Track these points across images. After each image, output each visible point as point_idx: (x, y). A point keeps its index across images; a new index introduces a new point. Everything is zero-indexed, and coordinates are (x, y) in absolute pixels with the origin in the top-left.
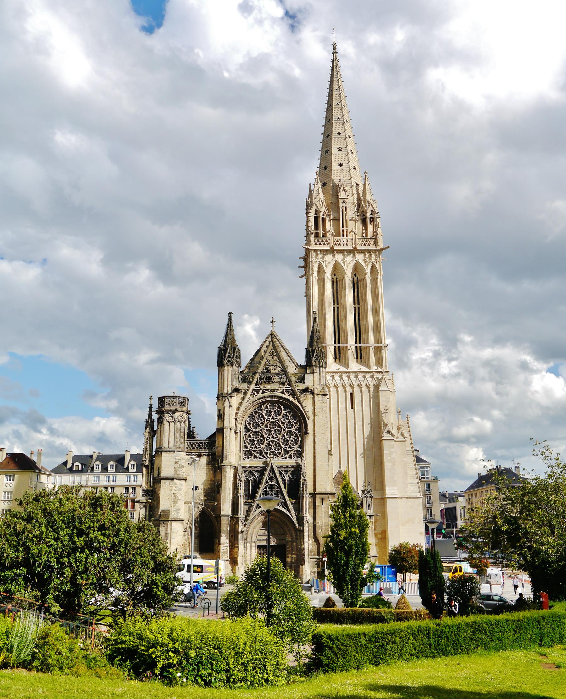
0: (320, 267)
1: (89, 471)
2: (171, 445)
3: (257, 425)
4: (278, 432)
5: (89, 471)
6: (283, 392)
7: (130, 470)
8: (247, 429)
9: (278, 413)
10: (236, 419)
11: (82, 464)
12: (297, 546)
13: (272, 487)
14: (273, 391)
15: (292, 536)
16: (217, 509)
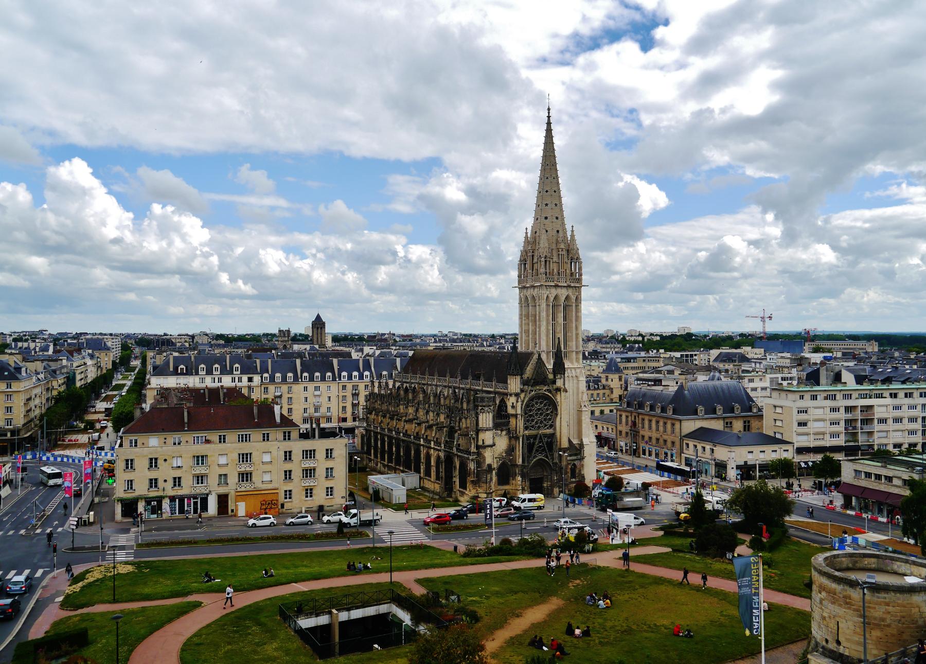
0: (547, 297)
1: (194, 374)
2: (491, 425)
3: (530, 411)
4: (541, 414)
5: (194, 374)
6: (545, 391)
7: (235, 373)
8: (526, 414)
9: (541, 403)
10: (522, 408)
11: (186, 367)
12: (551, 478)
13: (540, 447)
14: (540, 390)
15: (547, 472)
16: (514, 460)
